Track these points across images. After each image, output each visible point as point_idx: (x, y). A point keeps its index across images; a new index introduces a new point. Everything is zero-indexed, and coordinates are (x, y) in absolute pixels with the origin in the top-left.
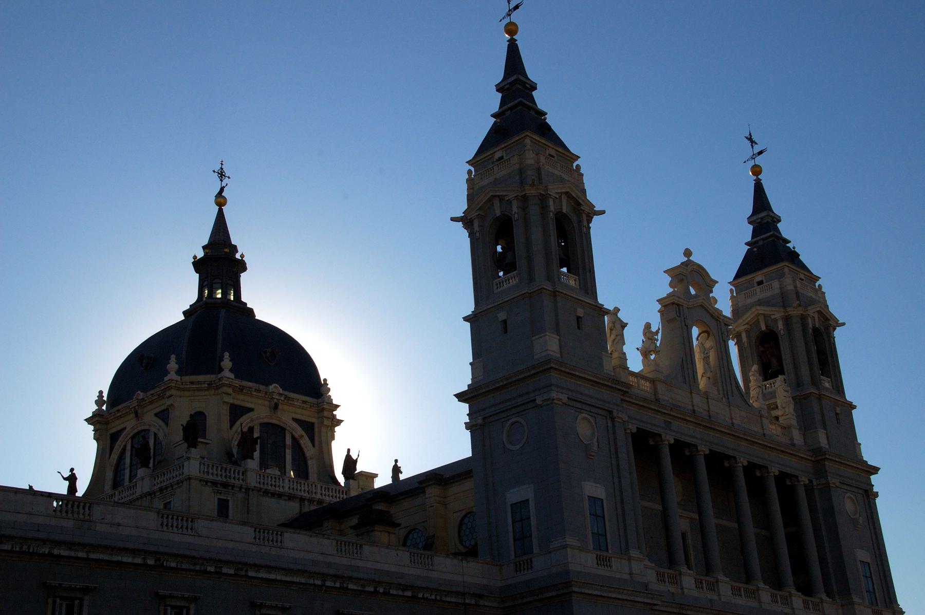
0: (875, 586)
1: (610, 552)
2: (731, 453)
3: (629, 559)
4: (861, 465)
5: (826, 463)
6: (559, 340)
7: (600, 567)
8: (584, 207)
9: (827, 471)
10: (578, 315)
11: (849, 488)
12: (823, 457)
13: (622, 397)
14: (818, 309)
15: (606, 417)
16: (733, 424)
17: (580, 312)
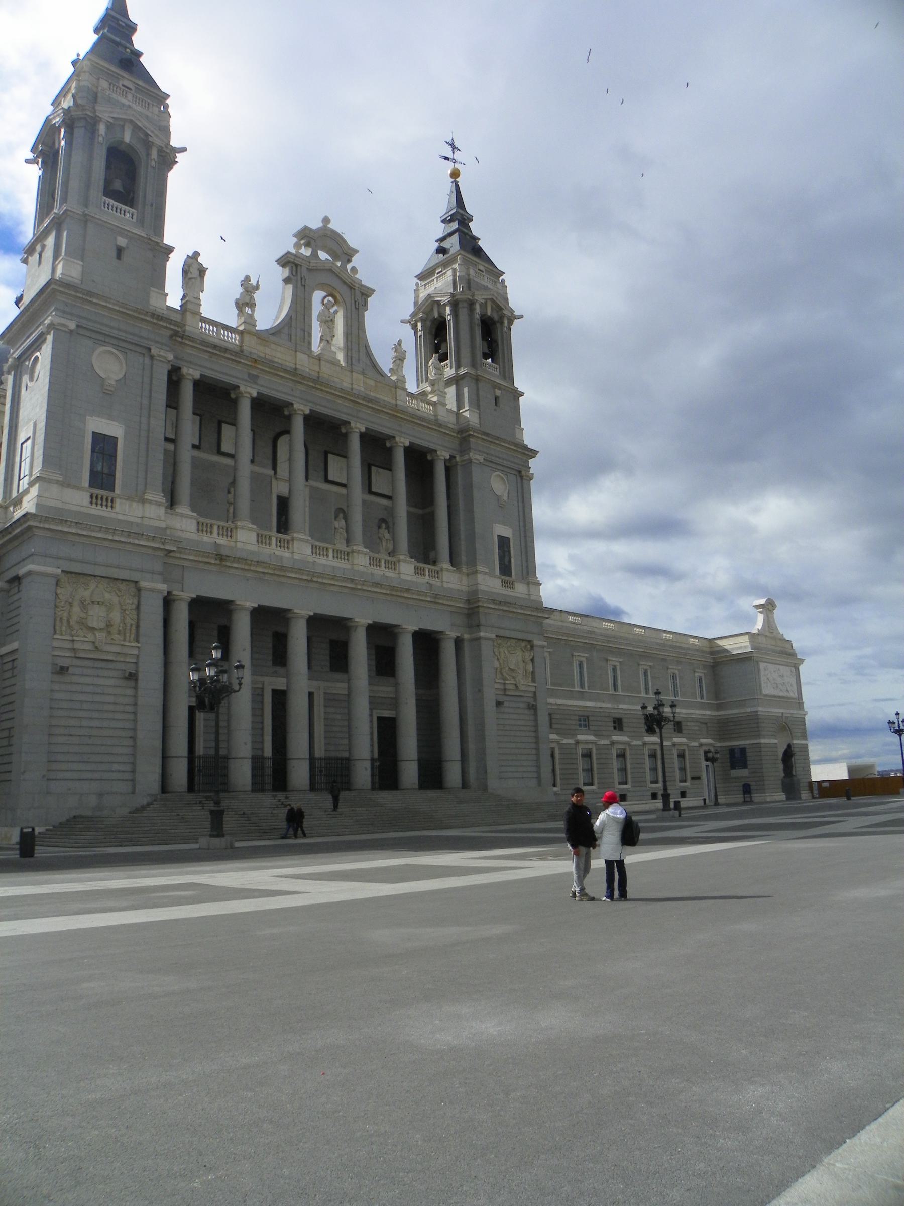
0: (513, 560)
1: (118, 491)
2: (344, 417)
3: (143, 501)
4: (515, 446)
5: (471, 439)
6: (83, 266)
7: (94, 506)
8: (154, 139)
9: (470, 448)
10: (118, 243)
11: (499, 467)
12: (467, 433)
13: (180, 339)
14: (491, 297)
16: (352, 389)
17: (122, 241)
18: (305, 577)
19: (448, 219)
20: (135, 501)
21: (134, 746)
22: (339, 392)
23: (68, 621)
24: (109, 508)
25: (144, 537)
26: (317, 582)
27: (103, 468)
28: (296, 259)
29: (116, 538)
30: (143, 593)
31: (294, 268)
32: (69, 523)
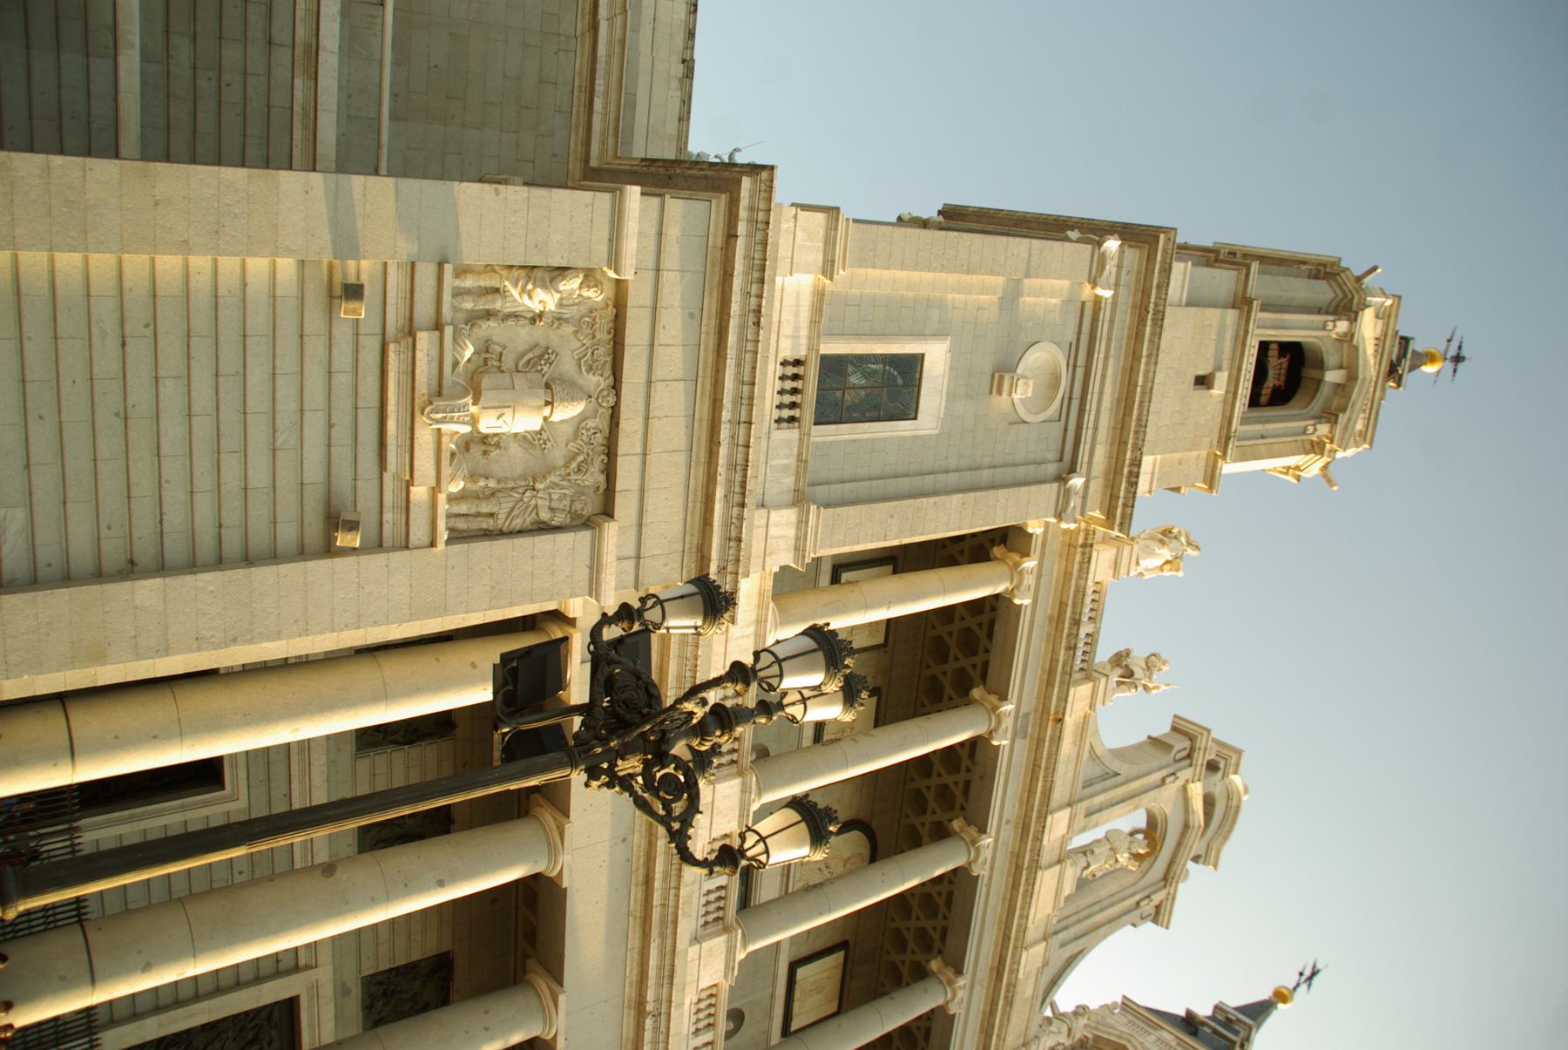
13: (1081, 541)
15: (1061, 460)
18: (650, 995)
19: (1230, 1016)
20: (797, 480)
21: (99, 575)
22: (1019, 926)
23: (489, 315)
24: (776, 414)
25: (736, 511)
26: (639, 1028)
27: (854, 387)
28: (1202, 753)
29: (725, 433)
30: (585, 536)
31: (1185, 753)
32: (754, 289)
